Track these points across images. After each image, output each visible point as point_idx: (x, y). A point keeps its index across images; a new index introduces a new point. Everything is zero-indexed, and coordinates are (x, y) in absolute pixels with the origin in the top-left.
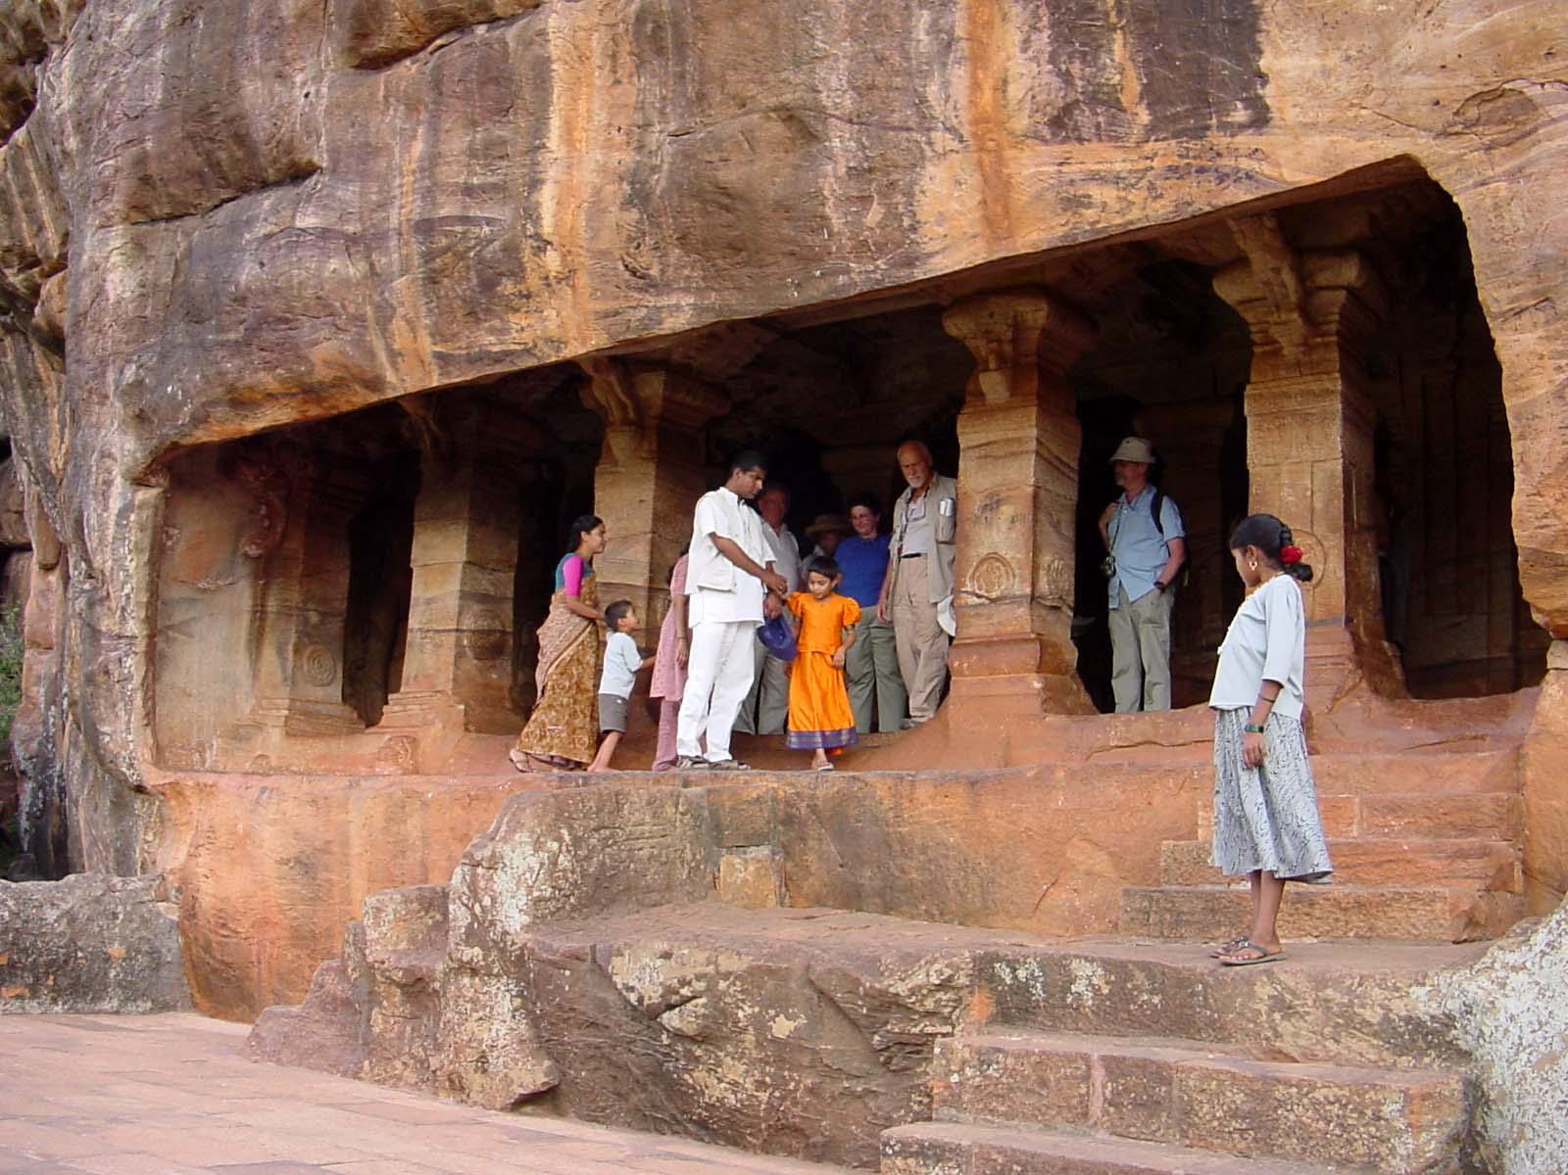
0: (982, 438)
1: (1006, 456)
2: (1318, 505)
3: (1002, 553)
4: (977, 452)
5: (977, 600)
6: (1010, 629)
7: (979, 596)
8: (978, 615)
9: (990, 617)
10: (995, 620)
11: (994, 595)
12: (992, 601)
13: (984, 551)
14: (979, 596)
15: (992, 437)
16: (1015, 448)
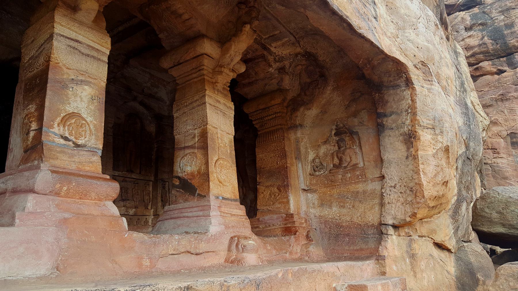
0: (73, 35)
1: (88, 55)
2: (229, 152)
3: (84, 116)
4: (68, 42)
5: (62, 141)
6: (88, 168)
7: (66, 139)
8: (62, 152)
9: (72, 156)
10: (76, 159)
11: (80, 142)
12: (77, 146)
13: (70, 109)
14: (66, 139)
15: (80, 38)
16: (95, 54)
